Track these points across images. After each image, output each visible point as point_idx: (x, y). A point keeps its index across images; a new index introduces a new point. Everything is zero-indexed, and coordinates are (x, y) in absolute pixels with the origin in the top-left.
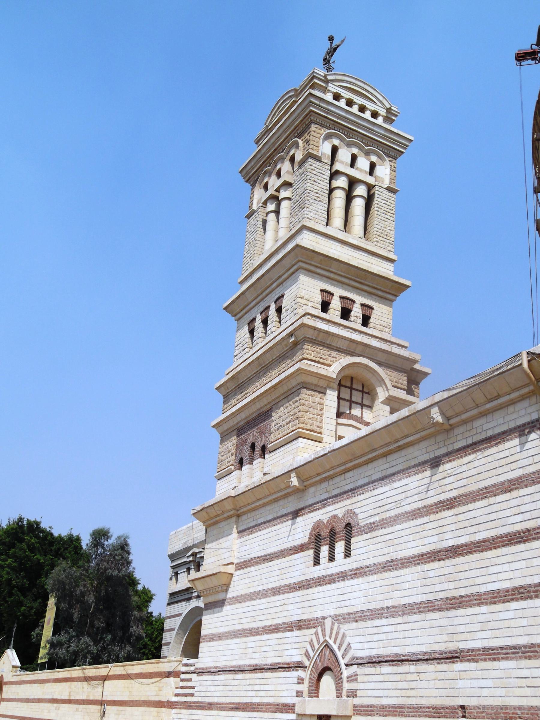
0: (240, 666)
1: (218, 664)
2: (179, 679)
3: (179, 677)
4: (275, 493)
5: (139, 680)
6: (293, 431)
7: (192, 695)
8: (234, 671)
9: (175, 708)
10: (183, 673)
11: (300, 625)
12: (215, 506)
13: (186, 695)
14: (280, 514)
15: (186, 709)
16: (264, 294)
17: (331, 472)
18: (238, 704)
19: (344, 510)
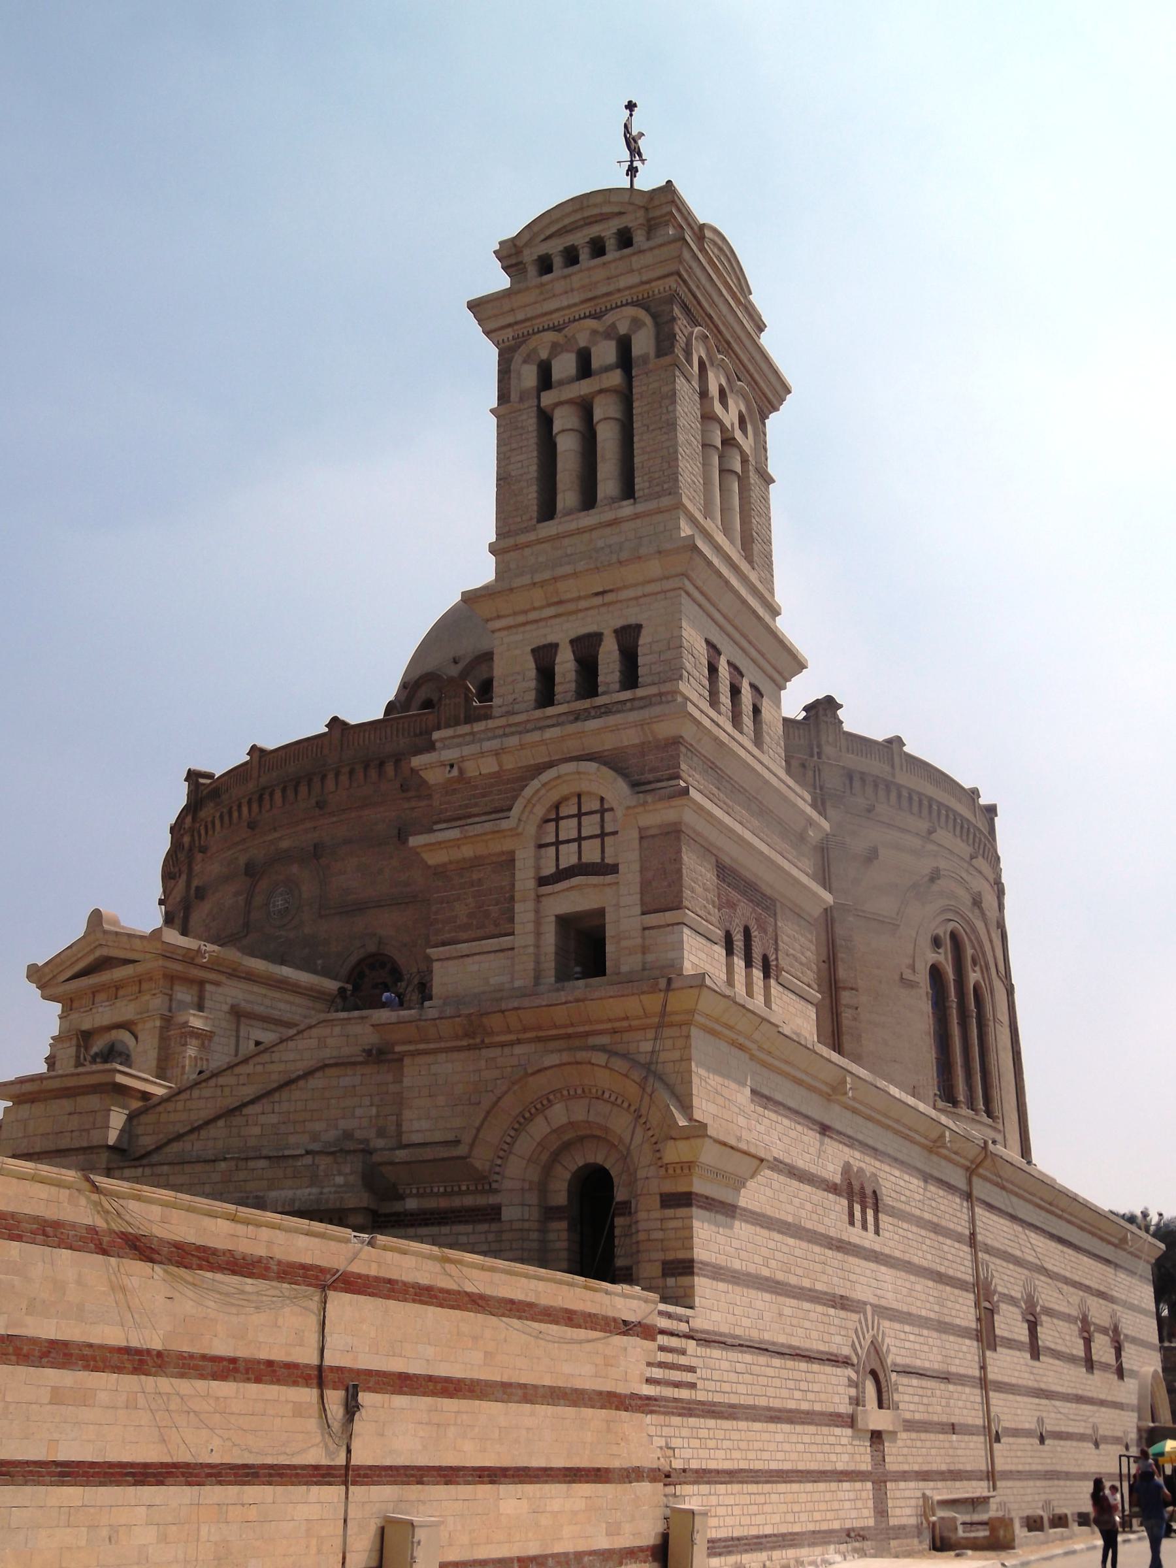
0: (774, 1344)
1: (738, 1331)
2: (648, 1344)
3: (654, 1340)
4: (807, 1073)
5: (535, 1325)
6: (809, 986)
7: (692, 1386)
8: (766, 1350)
9: (652, 1412)
10: (663, 1332)
11: (842, 1303)
12: (749, 1015)
13: (678, 1385)
14: (803, 1110)
15: (680, 1415)
16: (737, 636)
17: (776, 1063)
18: (780, 1410)
19: (874, 1170)
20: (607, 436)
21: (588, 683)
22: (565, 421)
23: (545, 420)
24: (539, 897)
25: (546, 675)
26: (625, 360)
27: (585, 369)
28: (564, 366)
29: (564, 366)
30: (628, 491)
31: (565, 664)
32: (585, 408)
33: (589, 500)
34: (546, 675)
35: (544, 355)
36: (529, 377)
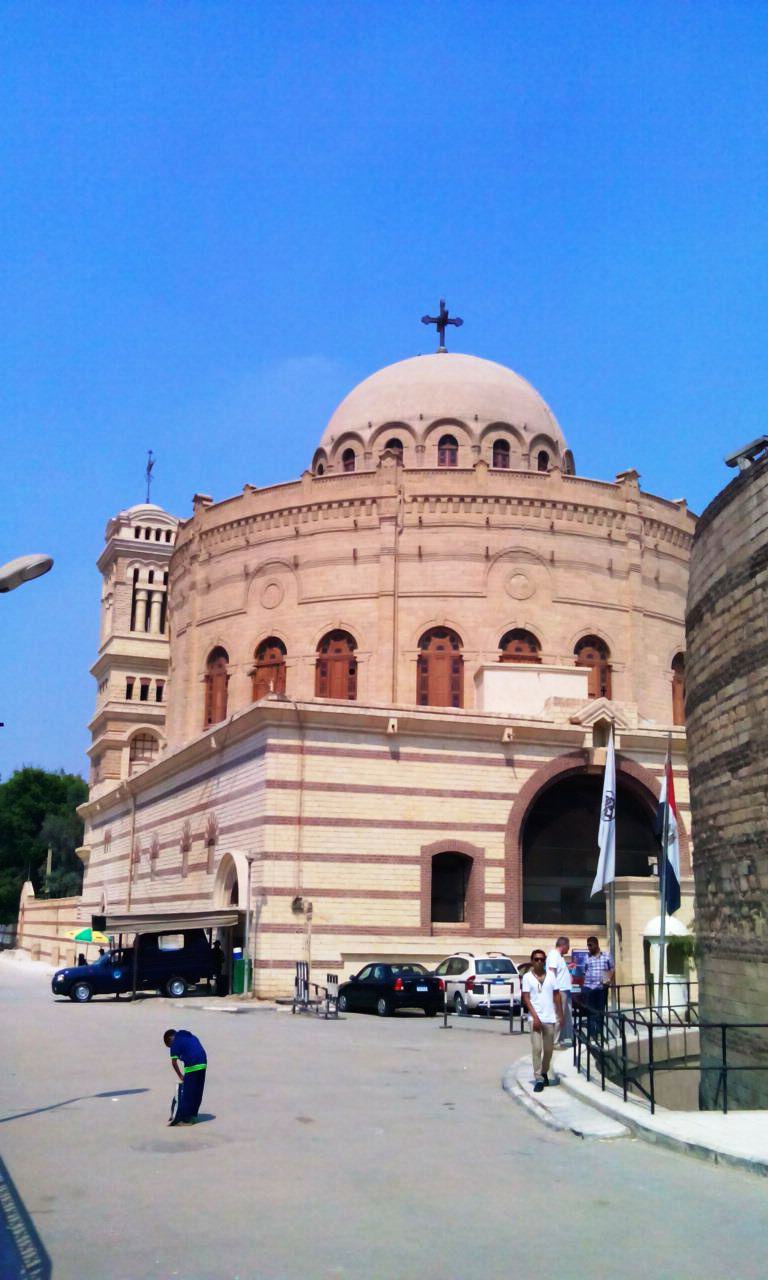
20: (156, 609)
21: (144, 695)
22: (142, 596)
23: (135, 592)
24: (130, 766)
25: (130, 688)
26: (165, 582)
27: (151, 580)
28: (144, 574)
29: (144, 574)
30: (162, 631)
31: (137, 685)
32: (150, 593)
33: (147, 628)
34: (130, 688)
35: (137, 566)
36: (130, 573)
